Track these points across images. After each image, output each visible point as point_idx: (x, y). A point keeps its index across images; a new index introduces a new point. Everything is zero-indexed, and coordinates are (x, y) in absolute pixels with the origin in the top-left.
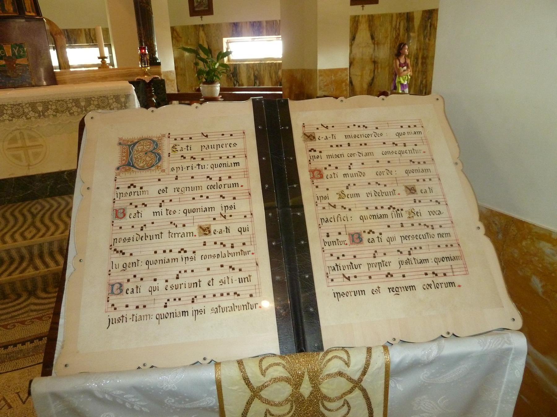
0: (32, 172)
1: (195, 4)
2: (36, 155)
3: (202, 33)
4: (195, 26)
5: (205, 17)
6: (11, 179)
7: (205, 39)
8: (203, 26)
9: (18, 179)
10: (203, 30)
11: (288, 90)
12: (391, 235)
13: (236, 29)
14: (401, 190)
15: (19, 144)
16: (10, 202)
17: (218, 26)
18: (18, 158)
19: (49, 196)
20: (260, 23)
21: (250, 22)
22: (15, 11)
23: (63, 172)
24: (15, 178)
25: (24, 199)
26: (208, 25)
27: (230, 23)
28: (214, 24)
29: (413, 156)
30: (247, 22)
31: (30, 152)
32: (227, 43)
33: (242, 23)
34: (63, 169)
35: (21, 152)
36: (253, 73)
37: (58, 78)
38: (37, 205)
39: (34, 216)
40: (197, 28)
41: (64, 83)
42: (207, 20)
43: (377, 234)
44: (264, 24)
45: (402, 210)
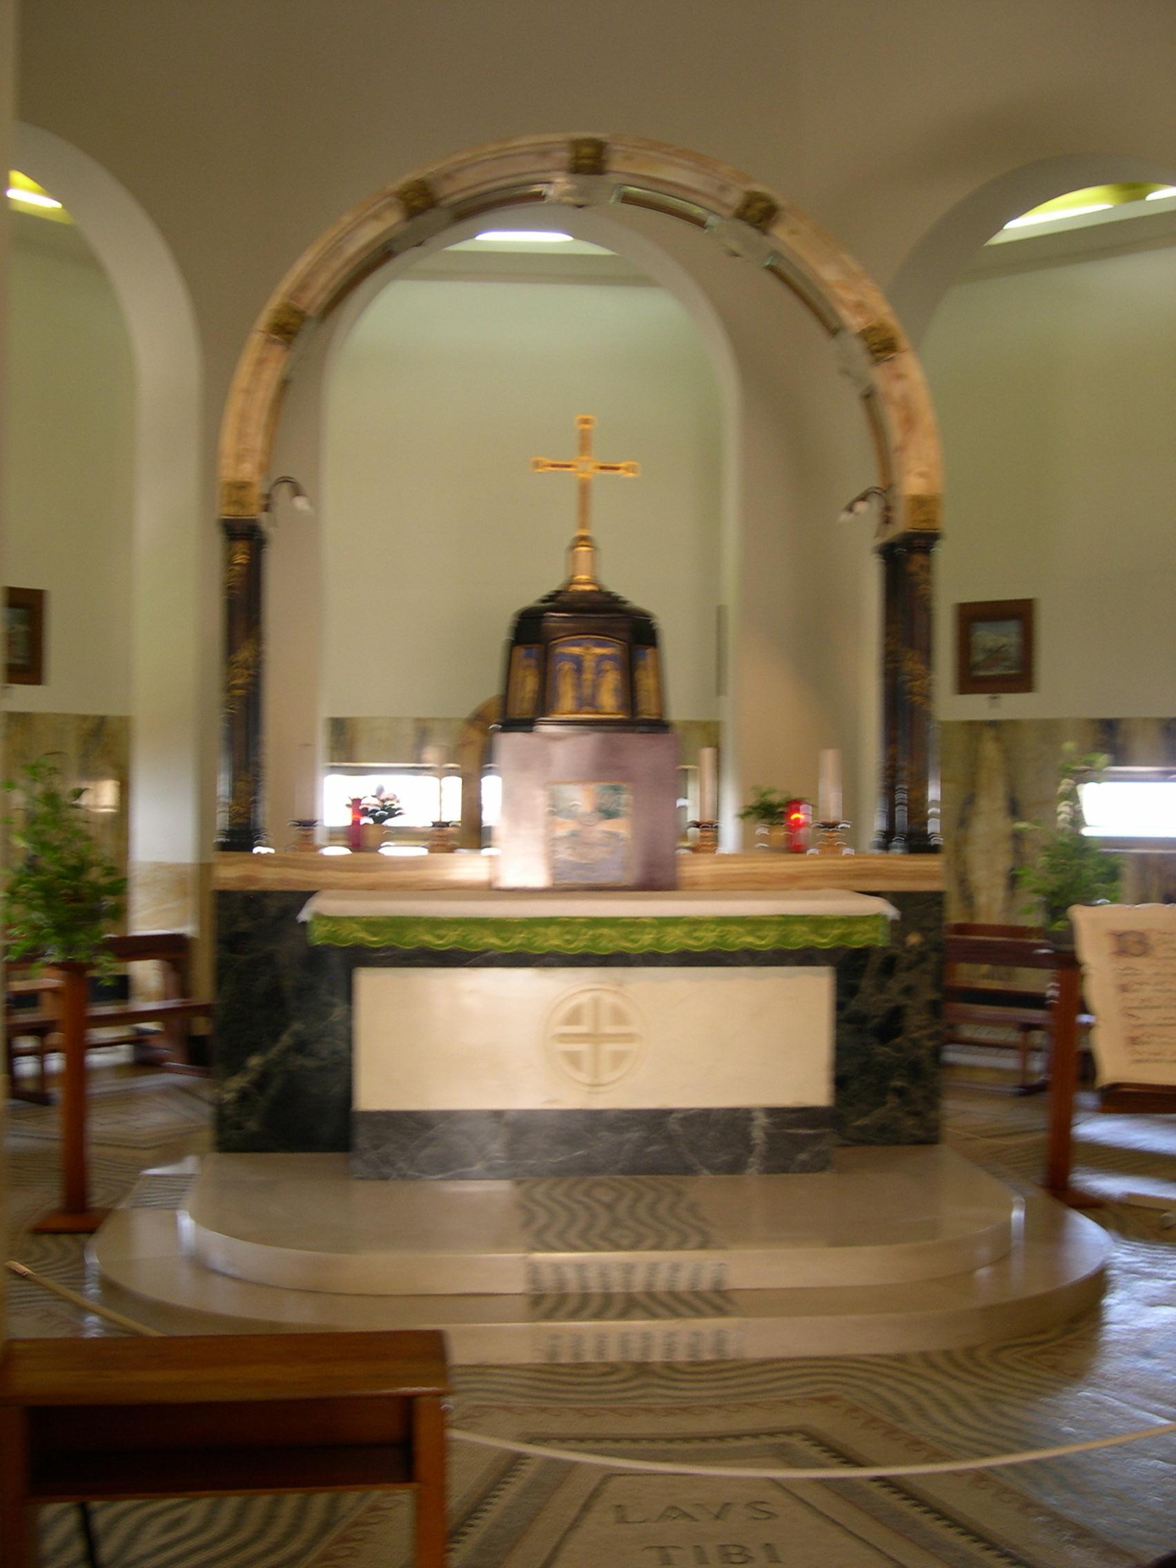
1: (978, 657)
2: (618, 1058)
3: (990, 749)
4: (971, 724)
8: (993, 724)
10: (997, 739)
13: (1112, 743)
17: (1049, 730)
18: (574, 1059)
21: (1160, 720)
23: (669, 1112)
24: (561, 1111)
26: (1014, 723)
27: (1094, 721)
30: (1146, 720)
31: (609, 1047)
35: (583, 1047)
39: (609, 1207)
40: (975, 728)
42: (1010, 706)
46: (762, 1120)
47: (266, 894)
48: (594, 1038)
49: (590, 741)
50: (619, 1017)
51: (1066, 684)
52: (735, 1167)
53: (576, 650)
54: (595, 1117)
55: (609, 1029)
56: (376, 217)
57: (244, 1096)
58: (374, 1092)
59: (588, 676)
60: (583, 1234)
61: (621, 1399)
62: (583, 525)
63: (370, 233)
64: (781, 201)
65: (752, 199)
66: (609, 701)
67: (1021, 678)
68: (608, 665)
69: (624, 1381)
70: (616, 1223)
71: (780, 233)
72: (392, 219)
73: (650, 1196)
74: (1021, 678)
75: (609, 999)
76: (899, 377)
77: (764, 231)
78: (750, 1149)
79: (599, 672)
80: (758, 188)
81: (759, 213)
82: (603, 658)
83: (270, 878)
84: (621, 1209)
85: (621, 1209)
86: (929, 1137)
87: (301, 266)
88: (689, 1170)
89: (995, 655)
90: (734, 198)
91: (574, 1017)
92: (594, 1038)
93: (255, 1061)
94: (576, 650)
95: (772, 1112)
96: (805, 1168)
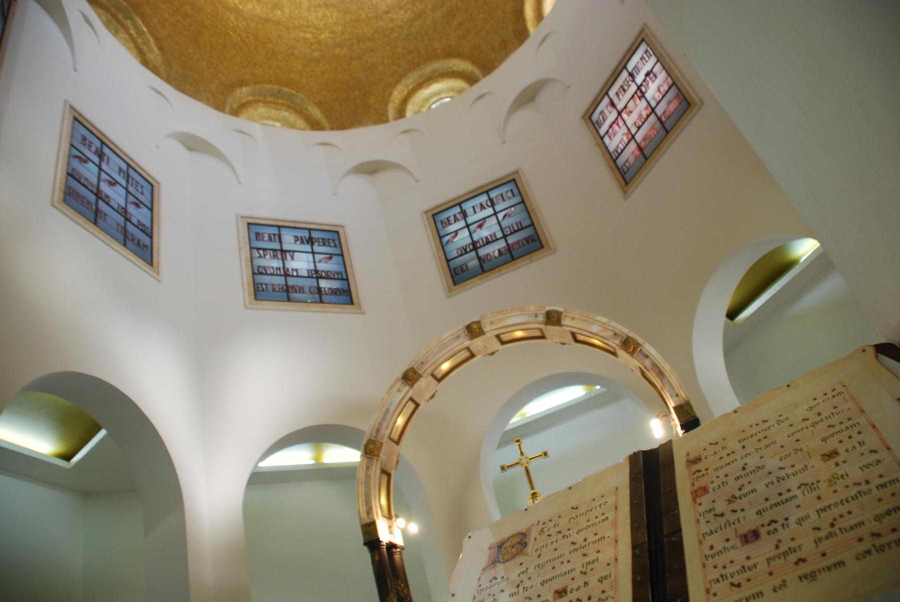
12: (801, 514)
14: (817, 461)
29: (830, 422)
43: (781, 521)
45: (818, 482)
56: (399, 391)
62: (532, 488)
71: (566, 321)
76: (647, 356)
80: (548, 308)
81: (553, 318)
90: (541, 318)
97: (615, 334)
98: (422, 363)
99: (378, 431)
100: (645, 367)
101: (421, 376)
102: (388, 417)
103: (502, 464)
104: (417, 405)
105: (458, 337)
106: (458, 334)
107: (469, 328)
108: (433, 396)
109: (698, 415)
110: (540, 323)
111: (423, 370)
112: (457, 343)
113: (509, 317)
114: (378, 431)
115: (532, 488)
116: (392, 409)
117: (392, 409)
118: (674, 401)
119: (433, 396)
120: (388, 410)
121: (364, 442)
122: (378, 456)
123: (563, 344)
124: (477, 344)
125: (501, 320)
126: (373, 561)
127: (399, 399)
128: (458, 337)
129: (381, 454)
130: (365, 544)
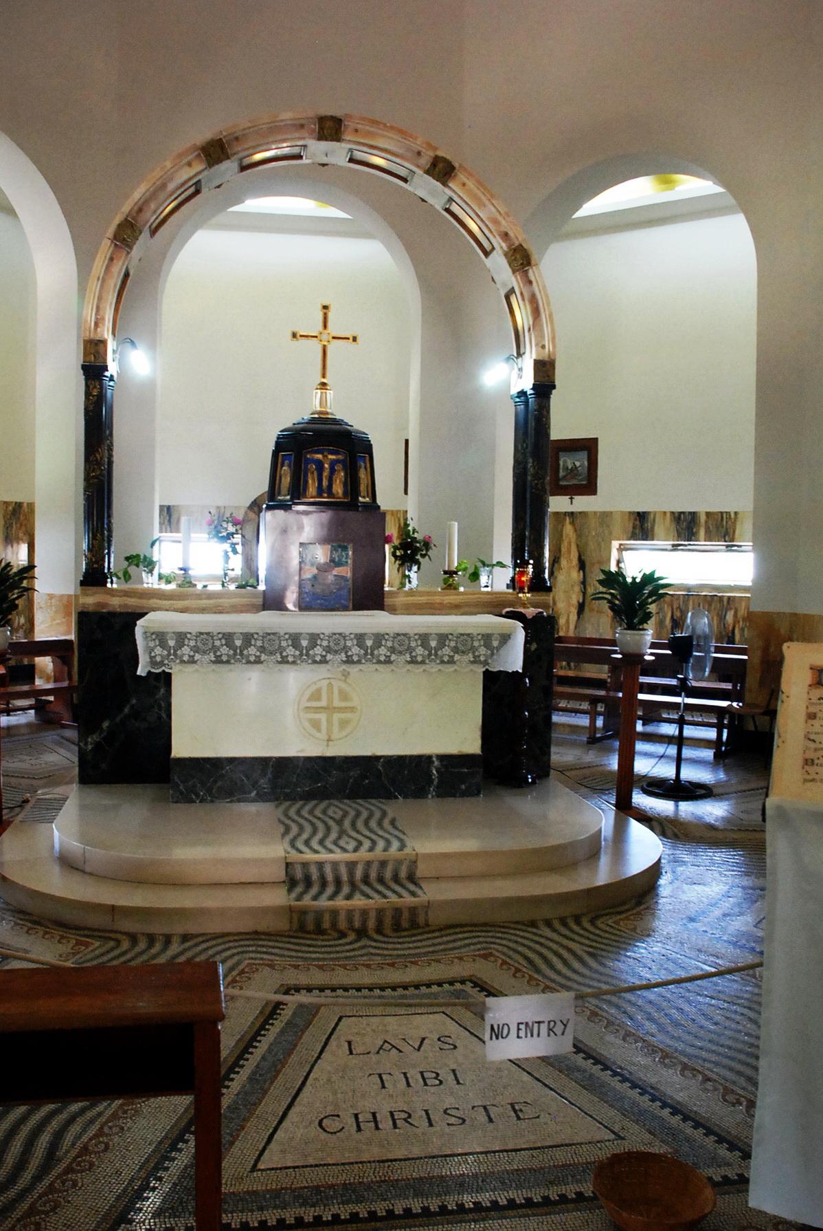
0: (330, 752)
1: (562, 473)
2: (343, 724)
3: (568, 529)
5: (577, 499)
6: (298, 758)
7: (573, 540)
9: (309, 759)
10: (572, 523)
11: (759, 653)
15: (323, 703)
16: (288, 797)
17: (605, 517)
18: (316, 725)
19: (349, 798)
20: (694, 515)
22: (345, 494)
23: (377, 758)
25: (307, 797)
28: (595, 513)
31: (337, 717)
32: (621, 549)
33: (655, 513)
34: (379, 753)
35: (323, 717)
36: (669, 615)
37: (387, 601)
38: (333, 808)
39: (339, 822)
41: (393, 610)
42: (581, 503)
44: (703, 518)
46: (436, 763)
47: (112, 614)
48: (329, 709)
49: (326, 516)
50: (344, 696)
51: (616, 492)
52: (420, 794)
53: (320, 456)
54: (331, 760)
55: (337, 703)
56: (189, 164)
57: (97, 746)
58: (183, 746)
59: (326, 474)
60: (321, 842)
61: (346, 958)
62: (324, 376)
63: (185, 174)
64: (456, 165)
65: (436, 161)
66: (338, 489)
67: (589, 487)
68: (338, 467)
69: (351, 943)
70: (342, 833)
72: (198, 167)
73: (365, 814)
74: (589, 487)
75: (337, 685)
76: (531, 282)
77: (445, 184)
78: (431, 782)
79: (332, 471)
80: (440, 153)
82: (337, 461)
83: (115, 603)
84: (347, 823)
85: (347, 823)
86: (543, 770)
87: (137, 194)
88: (390, 796)
89: (573, 472)
91: (316, 696)
92: (329, 709)
93: (106, 725)
94: (320, 456)
95: (443, 758)
96: (464, 794)
97: (506, 234)
98: (237, 139)
99: (140, 210)
100: (522, 294)
101: (228, 158)
102: (162, 196)
103: (295, 330)
104: (197, 192)
105: (302, 126)
106: (302, 122)
107: (322, 120)
108: (218, 187)
109: (557, 383)
110: (418, 166)
111: (236, 149)
112: (297, 135)
113: (383, 136)
114: (140, 210)
115: (324, 376)
116: (171, 186)
117: (171, 186)
118: (538, 354)
119: (218, 187)
120: (164, 186)
121: (117, 220)
122: (131, 248)
123: (423, 200)
124: (318, 149)
125: (369, 134)
126: (88, 394)
127: (185, 177)
128: (302, 126)
129: (135, 247)
130: (84, 367)
